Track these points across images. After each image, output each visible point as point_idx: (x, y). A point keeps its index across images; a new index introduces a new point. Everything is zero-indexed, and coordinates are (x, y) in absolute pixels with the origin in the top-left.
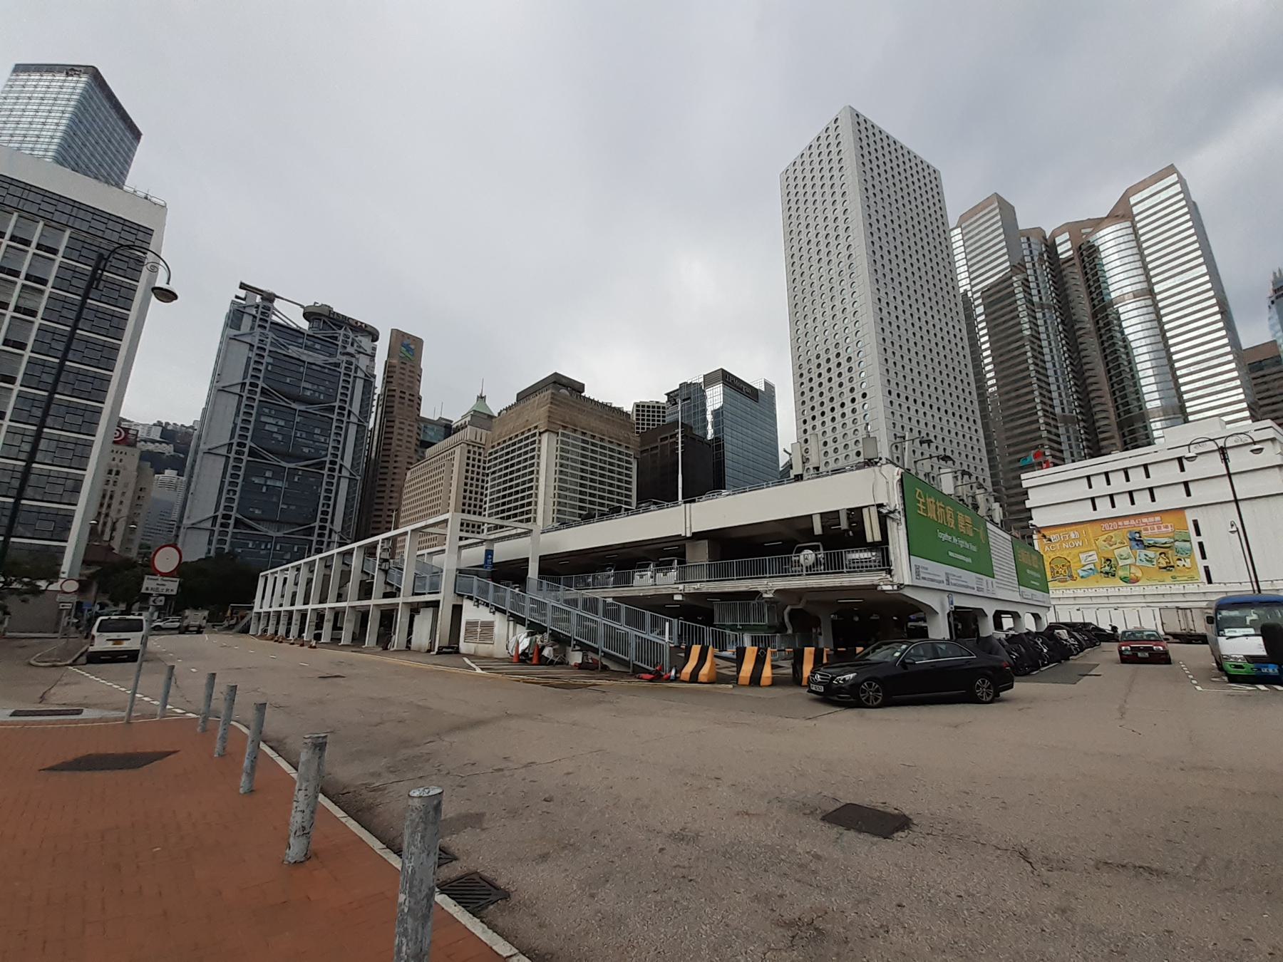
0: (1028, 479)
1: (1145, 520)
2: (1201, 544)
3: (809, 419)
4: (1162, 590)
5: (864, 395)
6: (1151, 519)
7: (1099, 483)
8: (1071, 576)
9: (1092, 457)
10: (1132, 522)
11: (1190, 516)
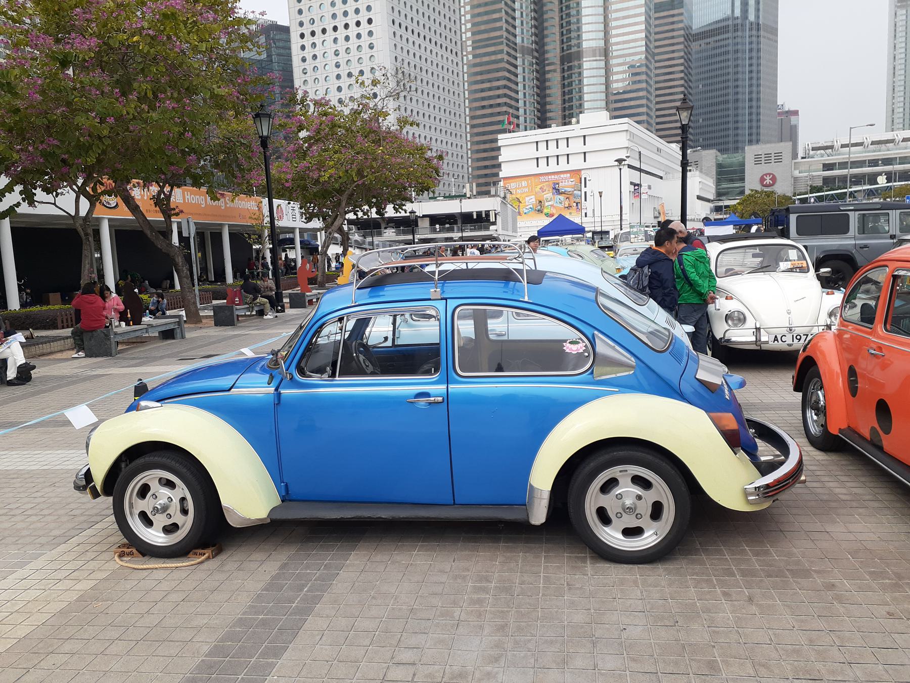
0: (503, 139)
1: (562, 176)
5: (370, 21)
9: (540, 127)
10: (556, 177)
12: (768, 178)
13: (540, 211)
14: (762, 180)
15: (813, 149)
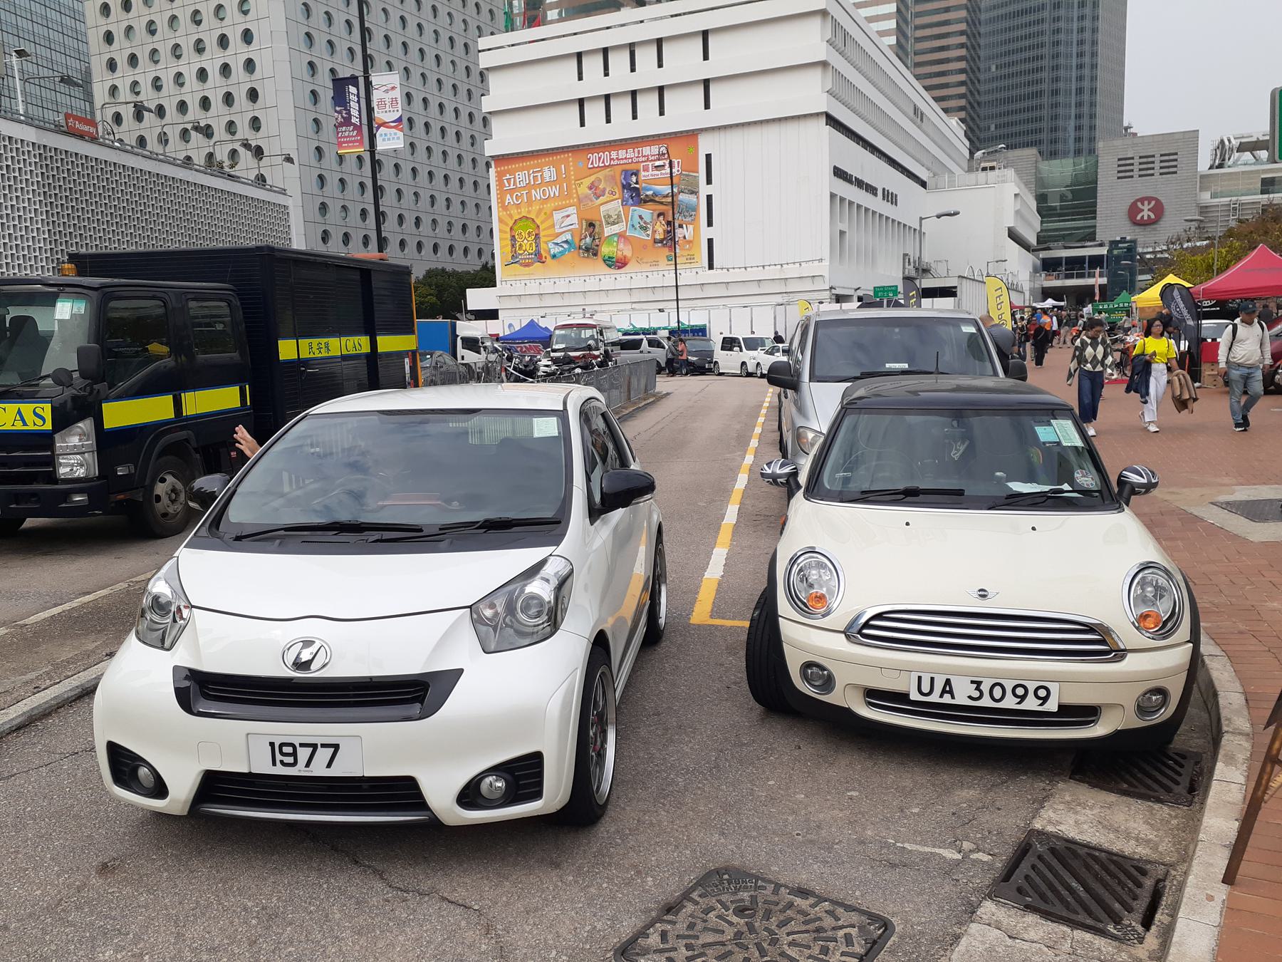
1: (646, 150)
2: (709, 198)
7: (593, 66)
8: (539, 257)
10: (631, 153)
11: (705, 145)
12: (1146, 207)
13: (592, 251)
14: (1133, 211)
15: (1242, 148)
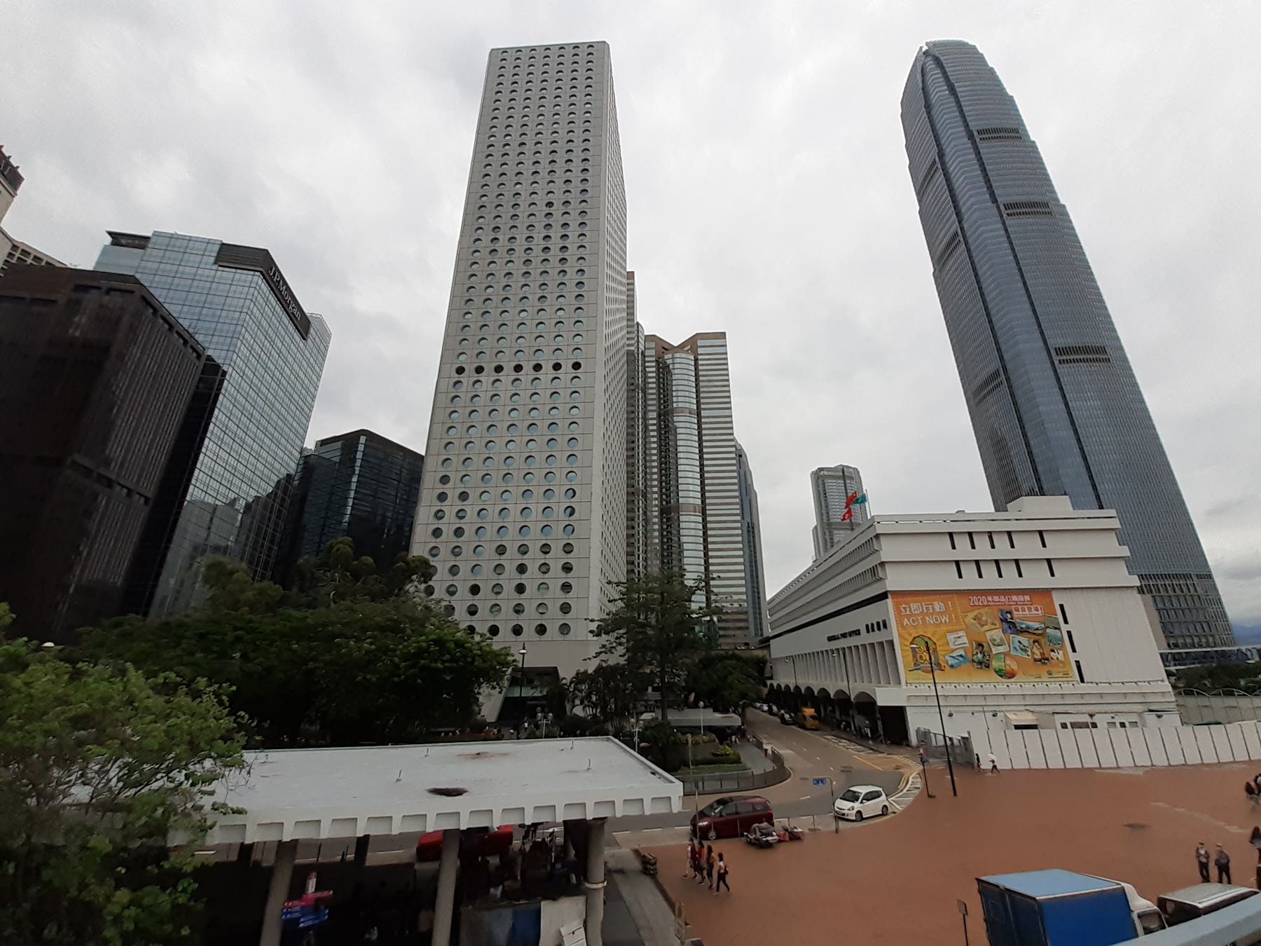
1: (1015, 598)
2: (1069, 633)
3: (470, 369)
4: (1041, 689)
5: (577, 366)
6: (1021, 598)
10: (1002, 599)
11: (1057, 599)
13: (984, 664)
